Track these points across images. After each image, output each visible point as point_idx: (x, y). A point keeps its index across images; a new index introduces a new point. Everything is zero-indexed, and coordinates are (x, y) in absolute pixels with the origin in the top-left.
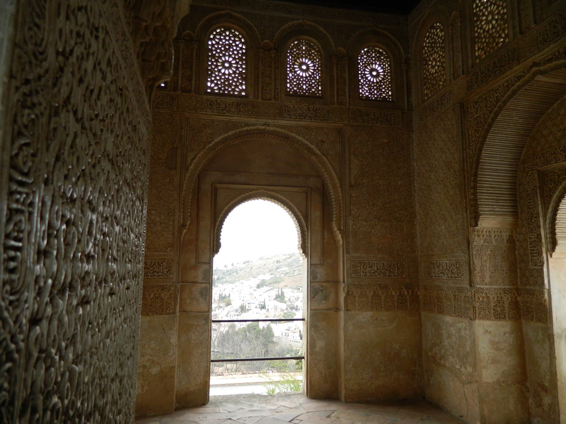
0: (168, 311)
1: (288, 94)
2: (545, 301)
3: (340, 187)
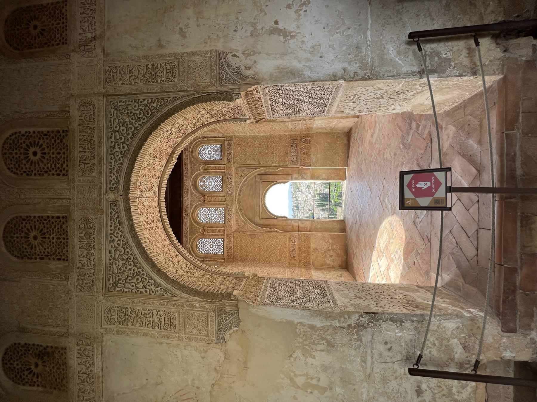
1: (222, 191)
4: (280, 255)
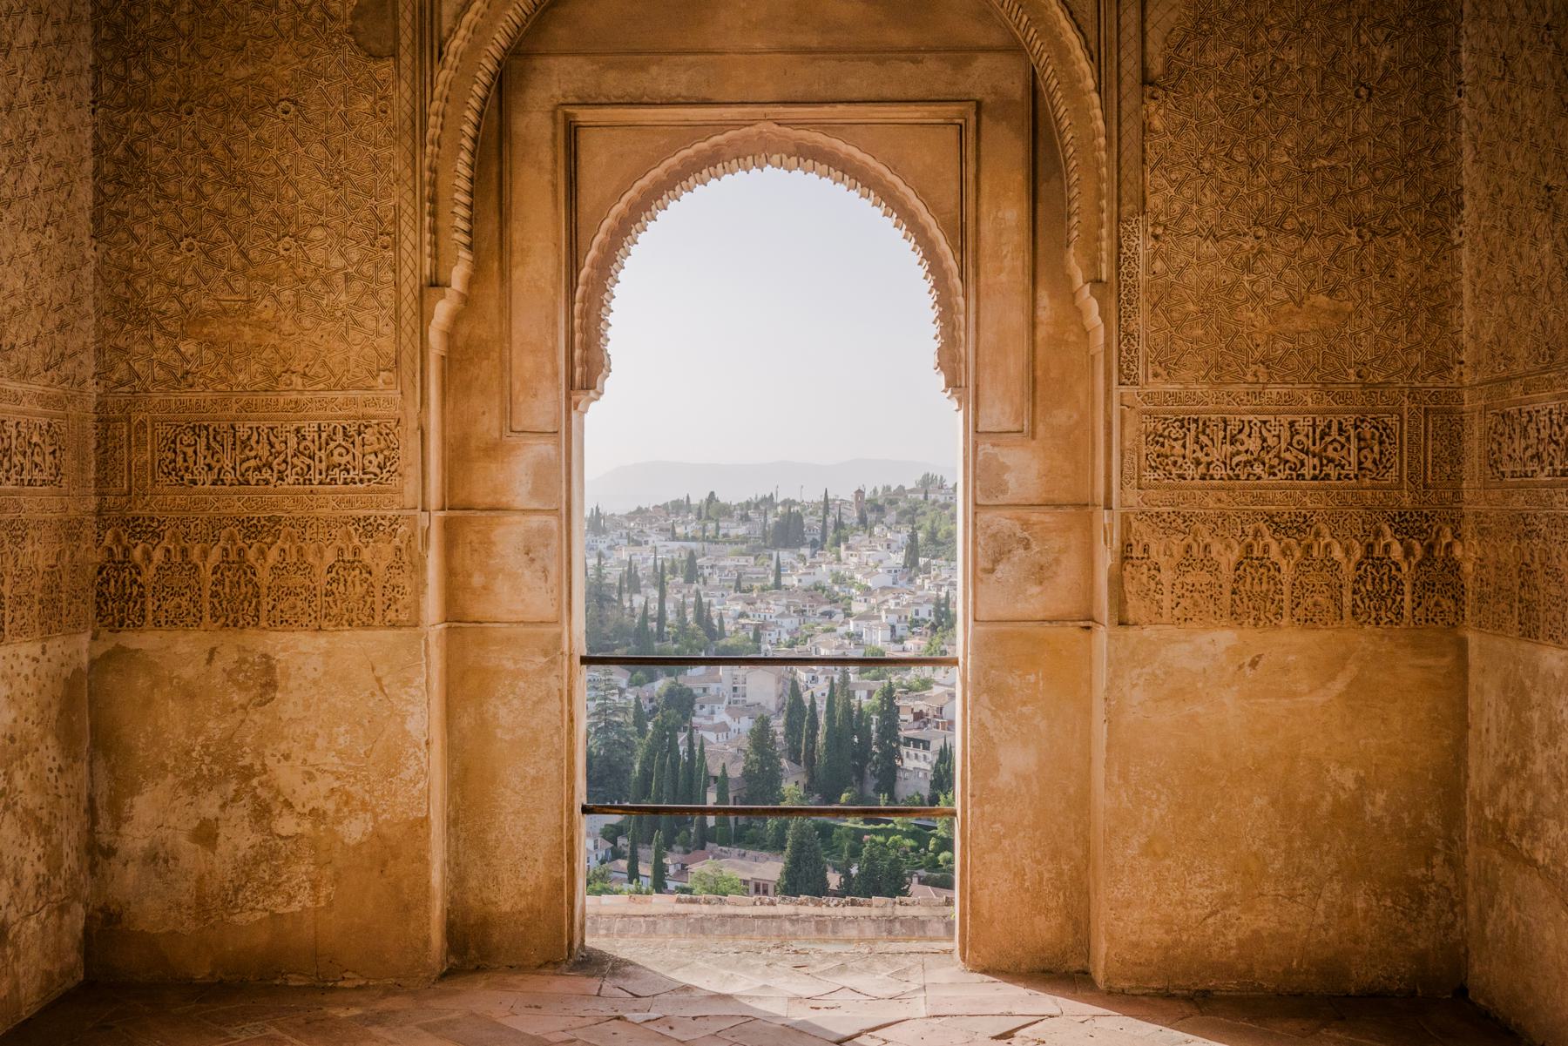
0: (391, 615)
3: (1098, 90)
4: (193, 320)
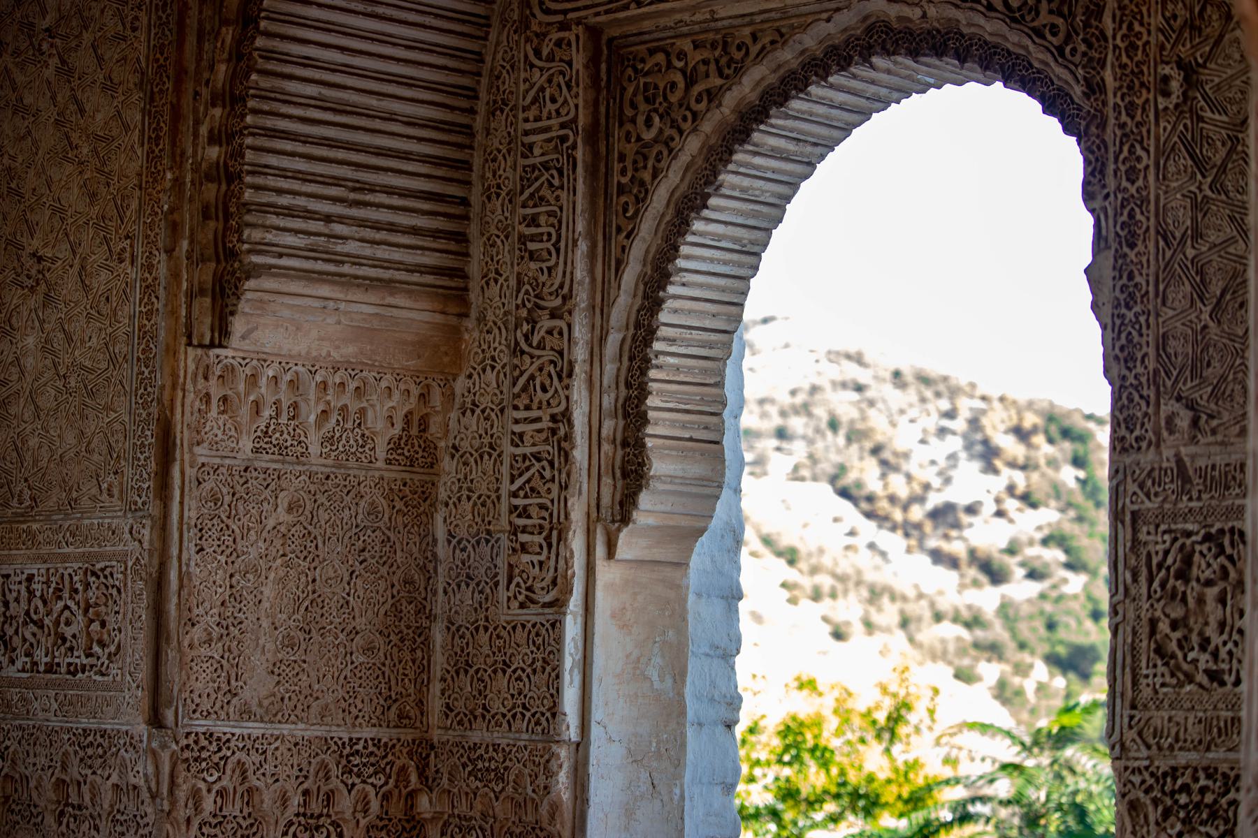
2: (555, 808)
